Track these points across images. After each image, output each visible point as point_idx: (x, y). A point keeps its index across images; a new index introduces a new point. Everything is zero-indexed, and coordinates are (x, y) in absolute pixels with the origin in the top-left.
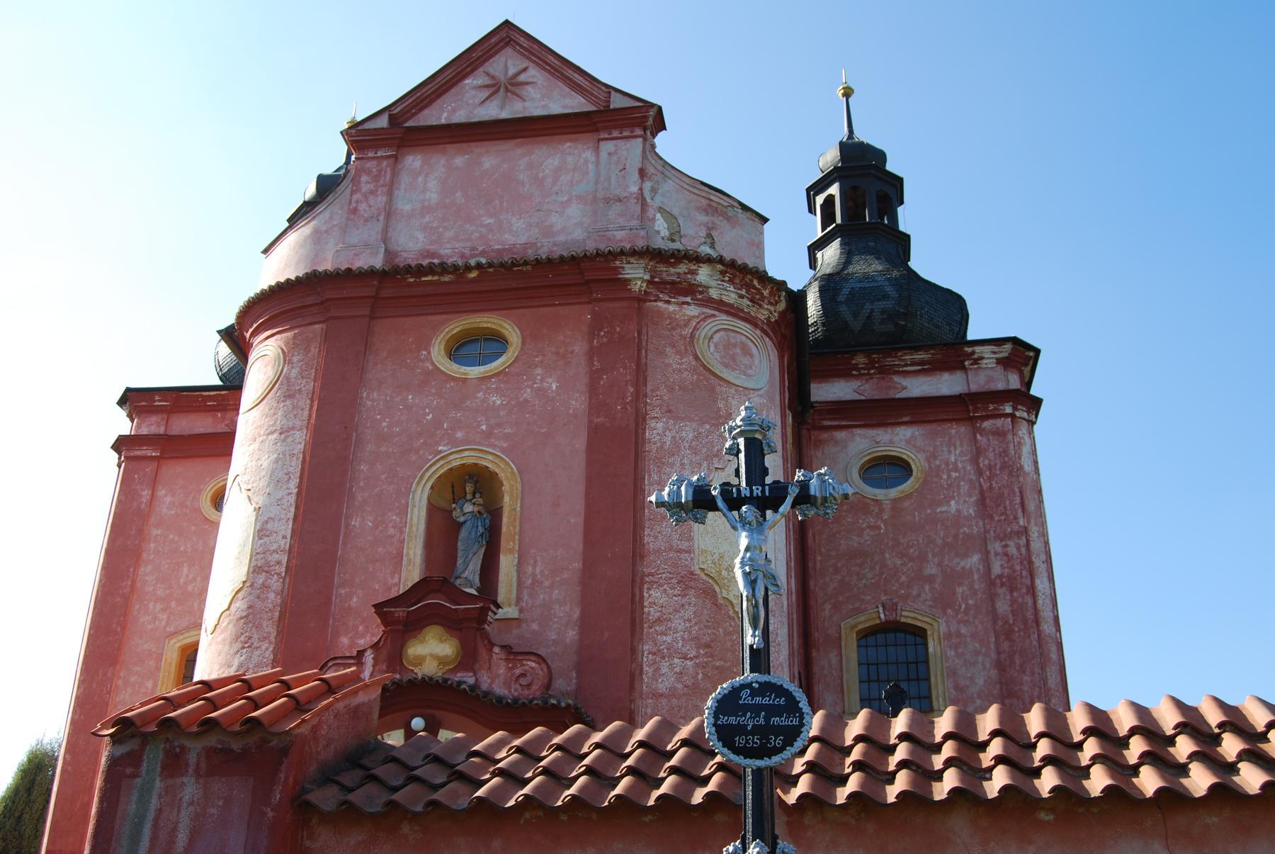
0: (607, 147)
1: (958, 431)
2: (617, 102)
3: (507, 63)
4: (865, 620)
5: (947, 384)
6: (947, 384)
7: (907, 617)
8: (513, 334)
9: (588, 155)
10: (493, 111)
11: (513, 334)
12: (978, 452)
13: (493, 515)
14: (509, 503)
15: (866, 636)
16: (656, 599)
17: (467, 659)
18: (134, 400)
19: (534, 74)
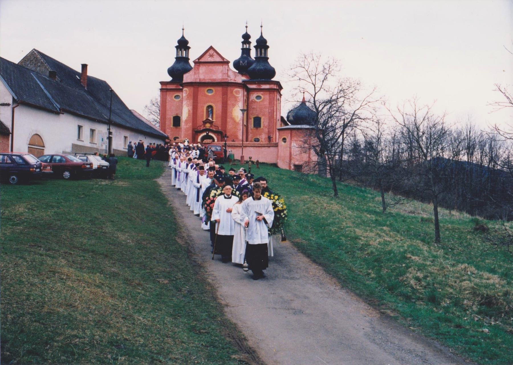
0: (224, 66)
1: (268, 93)
2: (225, 60)
3: (211, 52)
4: (254, 116)
5: (267, 87)
6: (267, 87)
7: (259, 116)
8: (214, 91)
9: (222, 67)
10: (210, 59)
11: (214, 91)
12: (270, 97)
13: (212, 110)
14: (214, 110)
15: (254, 118)
16: (228, 120)
17: (211, 127)
18: (162, 83)
19: (215, 54)
